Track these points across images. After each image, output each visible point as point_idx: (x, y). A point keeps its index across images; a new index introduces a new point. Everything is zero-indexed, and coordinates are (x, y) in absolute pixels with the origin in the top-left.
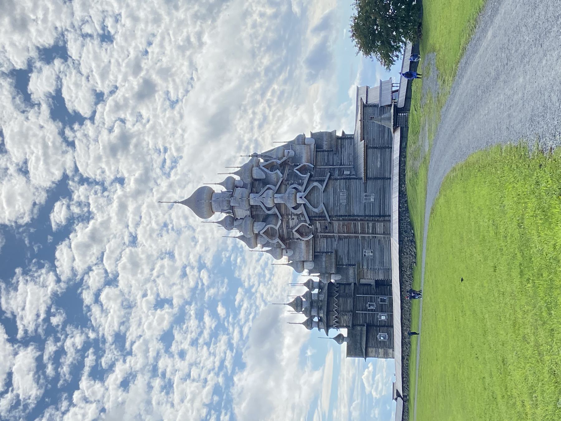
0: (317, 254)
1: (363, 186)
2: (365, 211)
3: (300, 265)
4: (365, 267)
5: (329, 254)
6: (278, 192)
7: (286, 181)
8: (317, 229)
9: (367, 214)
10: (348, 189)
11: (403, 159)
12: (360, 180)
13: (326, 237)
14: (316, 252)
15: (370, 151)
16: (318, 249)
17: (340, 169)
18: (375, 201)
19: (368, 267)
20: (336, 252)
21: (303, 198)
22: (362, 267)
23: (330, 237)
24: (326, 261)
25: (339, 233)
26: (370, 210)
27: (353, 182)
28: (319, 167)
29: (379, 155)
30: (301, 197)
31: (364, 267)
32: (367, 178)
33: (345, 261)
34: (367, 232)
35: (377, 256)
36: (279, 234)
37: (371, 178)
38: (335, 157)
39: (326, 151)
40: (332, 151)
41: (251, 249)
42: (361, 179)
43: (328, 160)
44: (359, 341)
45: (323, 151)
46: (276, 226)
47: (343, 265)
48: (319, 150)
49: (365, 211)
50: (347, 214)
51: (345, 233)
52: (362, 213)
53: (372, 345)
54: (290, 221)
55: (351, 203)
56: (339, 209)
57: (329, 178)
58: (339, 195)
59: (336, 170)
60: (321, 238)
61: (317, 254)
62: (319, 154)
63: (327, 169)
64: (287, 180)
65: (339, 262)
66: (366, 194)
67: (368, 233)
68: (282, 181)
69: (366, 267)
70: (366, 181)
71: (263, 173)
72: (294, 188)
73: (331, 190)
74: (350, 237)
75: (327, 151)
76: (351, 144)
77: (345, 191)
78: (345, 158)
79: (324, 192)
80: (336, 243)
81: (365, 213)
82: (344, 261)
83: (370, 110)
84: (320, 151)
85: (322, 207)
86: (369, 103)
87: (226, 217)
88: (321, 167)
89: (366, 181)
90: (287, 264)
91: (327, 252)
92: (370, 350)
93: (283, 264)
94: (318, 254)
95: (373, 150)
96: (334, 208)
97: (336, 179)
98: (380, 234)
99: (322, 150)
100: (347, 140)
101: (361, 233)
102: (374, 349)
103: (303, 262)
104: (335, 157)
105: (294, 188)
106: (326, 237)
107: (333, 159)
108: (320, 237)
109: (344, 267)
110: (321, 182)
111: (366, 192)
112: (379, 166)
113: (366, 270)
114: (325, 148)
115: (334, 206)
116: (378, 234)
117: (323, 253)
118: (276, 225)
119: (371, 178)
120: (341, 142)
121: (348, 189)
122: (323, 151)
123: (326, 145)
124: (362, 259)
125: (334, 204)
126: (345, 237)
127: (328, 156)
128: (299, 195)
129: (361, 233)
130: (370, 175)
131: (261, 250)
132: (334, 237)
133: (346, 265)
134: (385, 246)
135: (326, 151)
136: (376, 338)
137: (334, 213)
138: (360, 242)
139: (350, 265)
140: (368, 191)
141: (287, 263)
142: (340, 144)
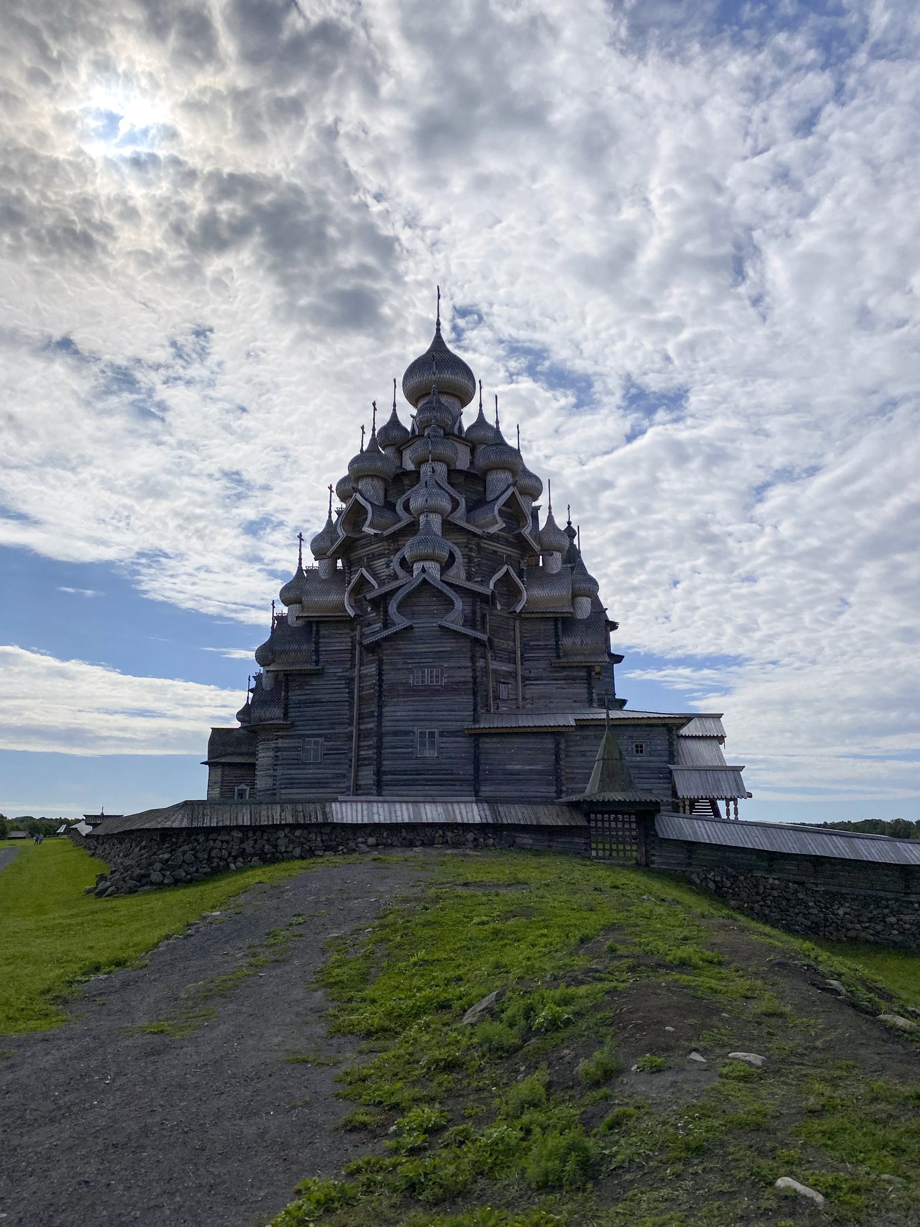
0: (314, 629)
1: (456, 726)
2: (395, 734)
3: (291, 595)
4: (281, 743)
5: (314, 658)
6: (449, 527)
7: (478, 545)
8: (369, 625)
9: (386, 739)
10: (451, 689)
11: (470, 836)
12: (471, 718)
13: (353, 648)
14: (317, 627)
15: (549, 744)
16: (326, 632)
17: (513, 675)
18: (417, 758)
19: (277, 749)
20: (319, 674)
21: (424, 575)
22: (282, 737)
23: (353, 657)
24: (300, 651)
25: (360, 677)
26: (395, 747)
27: (466, 700)
28: (517, 625)
29: (539, 767)
30: (424, 570)
31: (280, 741)
32: (477, 736)
33: (295, 695)
34: (362, 744)
35: (308, 771)
36: (358, 540)
37: (477, 747)
38: (543, 664)
39: (557, 642)
40: (558, 657)
41: (334, 489)
42: (475, 720)
43: (538, 648)
44: (237, 750)
45: (557, 635)
46: (369, 526)
47: (287, 692)
48: (560, 626)
49: (395, 734)
50: (385, 687)
51: (359, 691)
52: (387, 726)
53: (227, 776)
54: (383, 561)
55: (414, 696)
56: (399, 666)
57: (476, 641)
58: (435, 667)
59: (512, 666)
60: (351, 637)
61: (314, 629)
62: (550, 626)
63: (512, 644)
64: (480, 549)
65: (294, 681)
66: (437, 735)
67: (359, 747)
68: (474, 534)
69: (280, 745)
70: (471, 735)
71: (498, 493)
72: (452, 556)
73: (448, 645)
74: (351, 705)
75: (557, 645)
76: (575, 701)
77: (445, 680)
78: (541, 687)
79: (441, 627)
80: (339, 671)
81: (388, 733)
82: (298, 692)
83: (660, 743)
84: (556, 628)
85: (401, 622)
86: (682, 741)
87: (406, 430)
88: (518, 631)
89: (471, 735)
90: (300, 569)
91: (317, 652)
92: (219, 771)
93: (300, 559)
94: (314, 632)
95: (553, 751)
96: (399, 654)
97: (473, 659)
98: (356, 776)
99: (560, 634)
100: (586, 691)
101: (359, 730)
102: (219, 779)
103: (300, 602)
104: (543, 664)
105: (452, 556)
106: (353, 648)
107: (538, 659)
108: (353, 634)
109: (283, 694)
110: (470, 621)
111: (442, 734)
112: (509, 767)
113: (273, 745)
114: (567, 642)
115: (404, 654)
116: (357, 771)
117: (317, 643)
118: (372, 525)
119: (477, 747)
120: (581, 678)
121: (451, 689)
122: (557, 635)
123: (574, 643)
124: (300, 736)
125: (411, 655)
126: (351, 693)
127: (545, 647)
128: (434, 569)
129: (359, 730)
130: (487, 744)
131: (333, 509)
132: (353, 666)
133: (287, 698)
134: (329, 790)
135: (557, 642)
136: (241, 783)
137: (387, 655)
138: (339, 730)
139: (286, 707)
140: (444, 739)
141: (304, 568)
142: (575, 674)
